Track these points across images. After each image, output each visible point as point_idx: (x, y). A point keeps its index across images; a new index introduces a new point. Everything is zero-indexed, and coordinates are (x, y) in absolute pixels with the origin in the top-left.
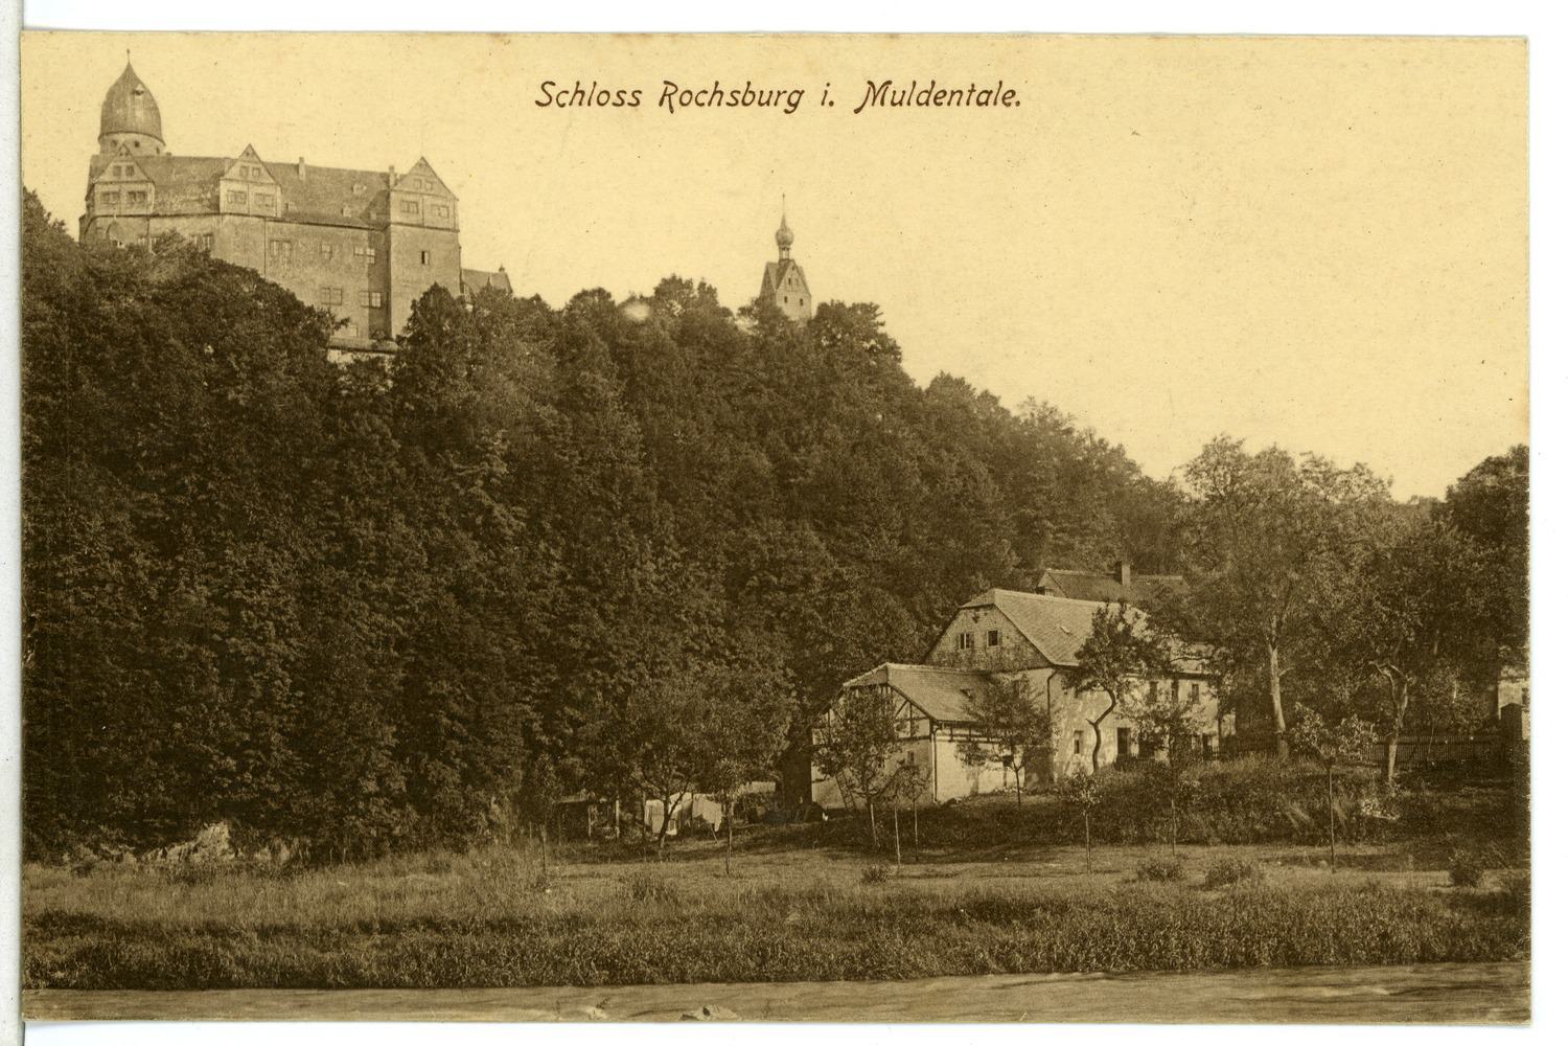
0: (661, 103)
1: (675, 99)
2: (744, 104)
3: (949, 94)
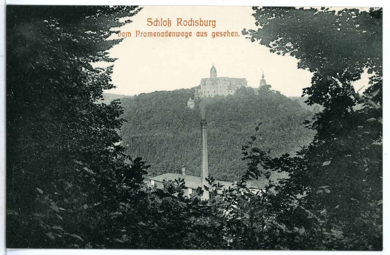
0: (178, 25)
1: (182, 23)
2: (201, 25)
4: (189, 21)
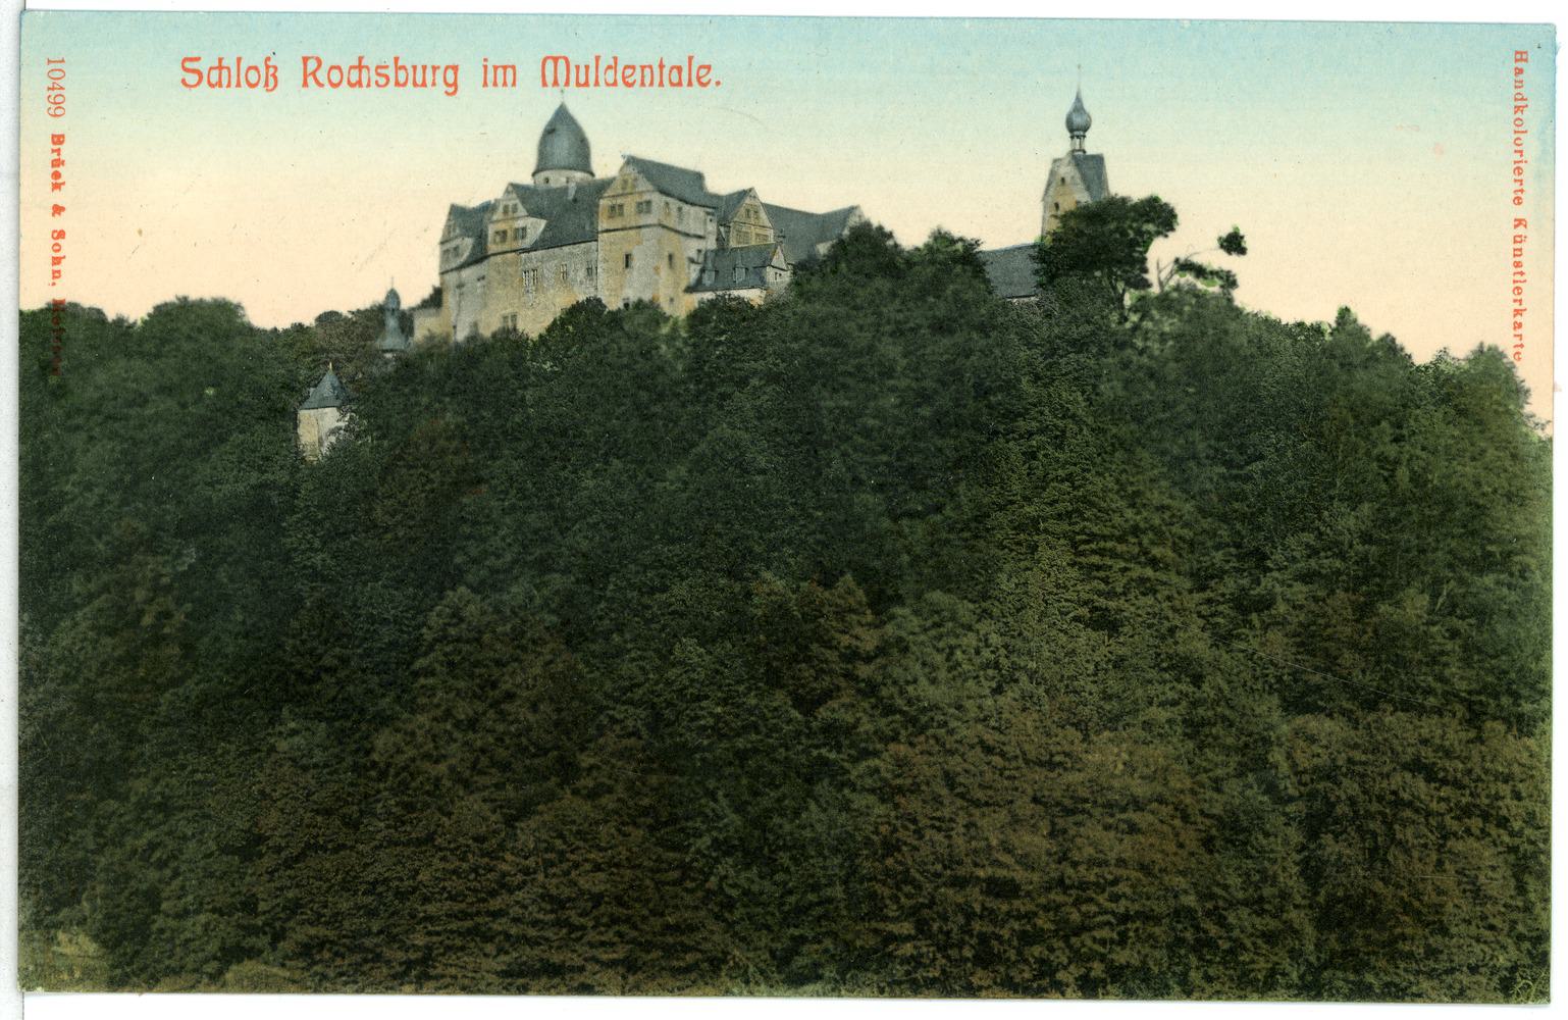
0: (305, 84)
1: (322, 75)
2: (397, 84)
3: (638, 70)
4: (351, 68)
